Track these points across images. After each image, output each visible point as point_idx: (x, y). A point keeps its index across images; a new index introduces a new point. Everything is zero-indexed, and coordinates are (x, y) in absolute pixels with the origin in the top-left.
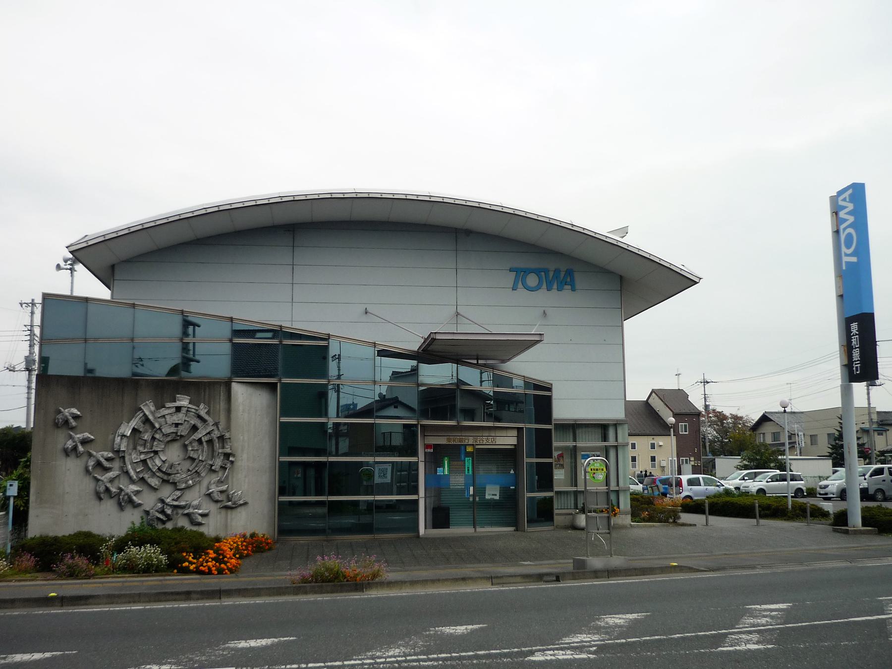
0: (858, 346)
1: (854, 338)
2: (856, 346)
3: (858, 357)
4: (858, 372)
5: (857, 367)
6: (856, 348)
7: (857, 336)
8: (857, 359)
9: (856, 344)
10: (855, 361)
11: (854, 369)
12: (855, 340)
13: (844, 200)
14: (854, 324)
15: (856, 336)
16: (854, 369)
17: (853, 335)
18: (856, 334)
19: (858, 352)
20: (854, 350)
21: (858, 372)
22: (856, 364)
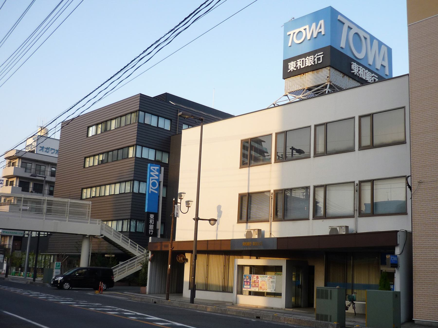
0: (153, 224)
1: (151, 220)
2: (152, 224)
3: (153, 228)
4: (151, 234)
5: (151, 232)
6: (151, 224)
7: (153, 220)
8: (152, 229)
9: (152, 222)
10: (151, 229)
11: (150, 232)
12: (152, 221)
13: (154, 169)
14: (152, 215)
15: (152, 220)
16: (150, 232)
17: (151, 219)
18: (153, 219)
19: (153, 226)
20: (150, 225)
21: (151, 234)
22: (150, 230)
